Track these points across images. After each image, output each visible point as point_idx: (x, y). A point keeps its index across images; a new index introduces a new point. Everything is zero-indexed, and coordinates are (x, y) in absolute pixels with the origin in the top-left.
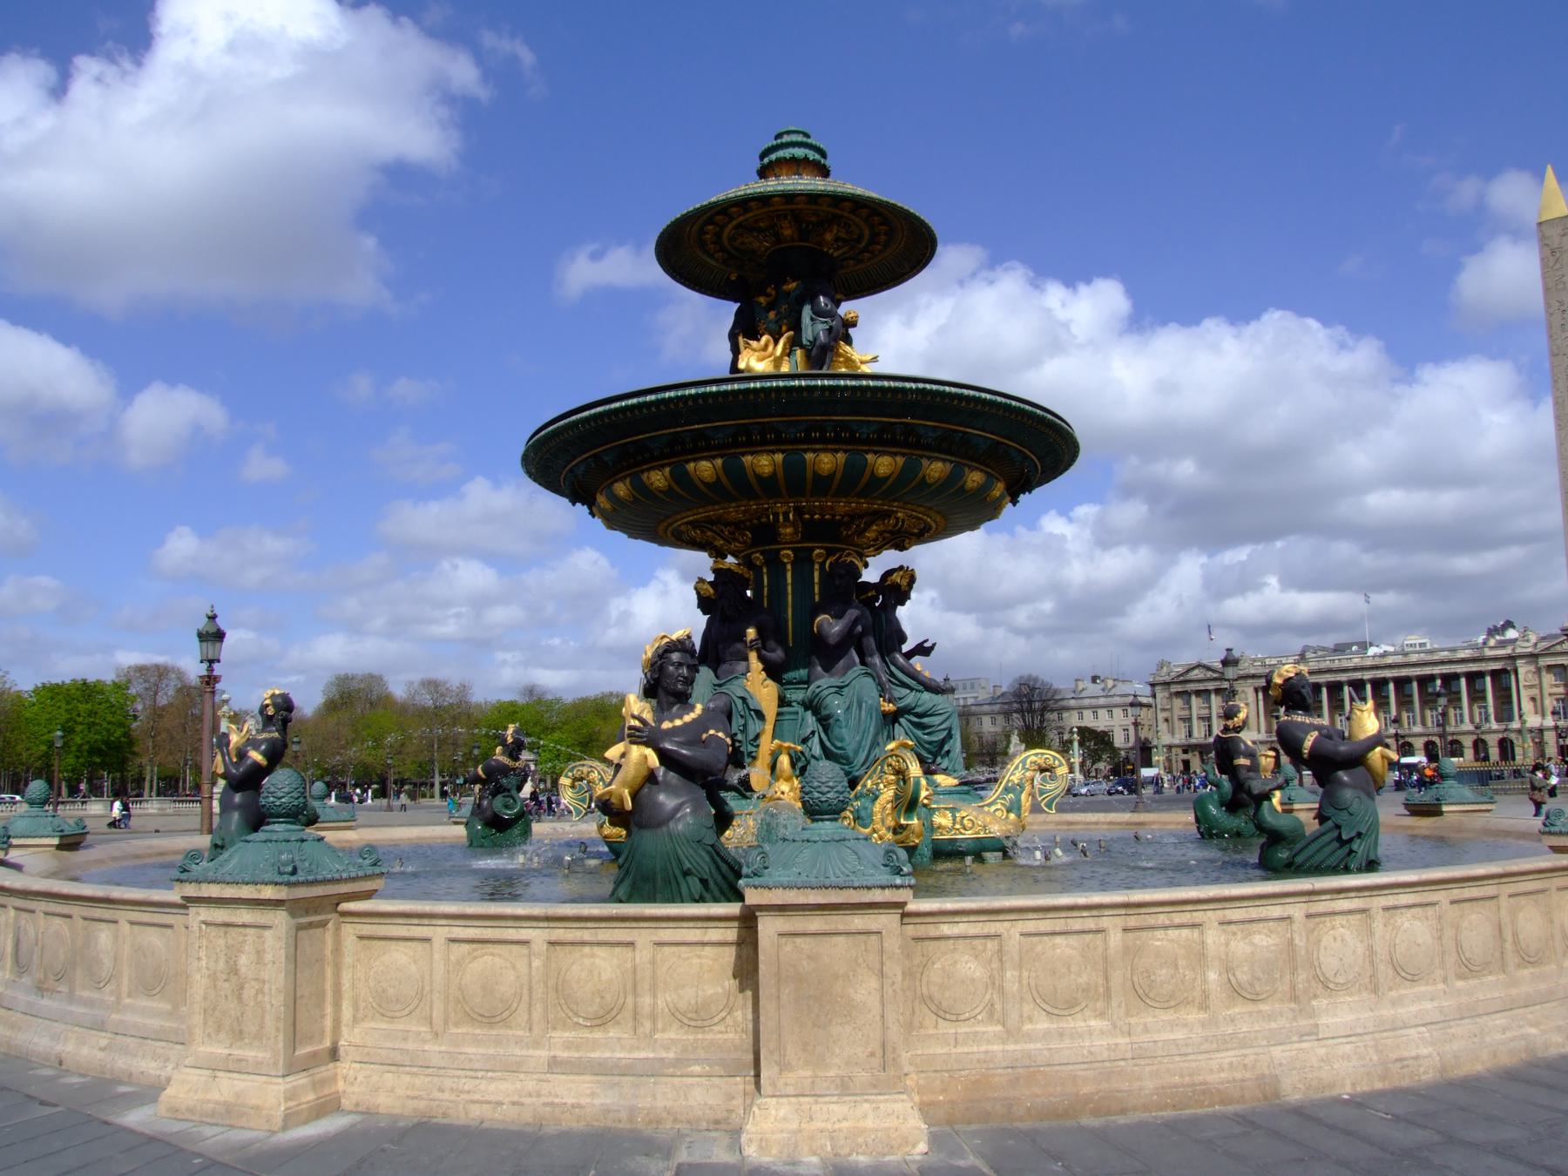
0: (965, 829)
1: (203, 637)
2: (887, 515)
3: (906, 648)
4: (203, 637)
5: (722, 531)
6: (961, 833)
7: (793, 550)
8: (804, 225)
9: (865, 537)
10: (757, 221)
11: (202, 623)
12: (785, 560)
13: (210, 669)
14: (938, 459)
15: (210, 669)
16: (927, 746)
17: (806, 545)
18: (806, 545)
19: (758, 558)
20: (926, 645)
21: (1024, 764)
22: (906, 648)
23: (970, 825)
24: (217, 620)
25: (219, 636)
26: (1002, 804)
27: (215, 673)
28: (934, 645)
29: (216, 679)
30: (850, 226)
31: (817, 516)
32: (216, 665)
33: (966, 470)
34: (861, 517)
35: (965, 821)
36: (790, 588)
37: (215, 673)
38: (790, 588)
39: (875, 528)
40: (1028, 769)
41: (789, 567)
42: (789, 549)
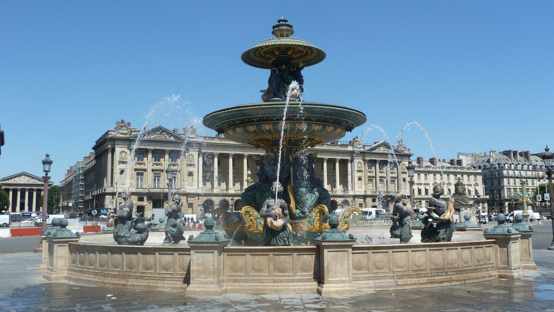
1: (45, 163)
4: (45, 163)
11: (44, 158)
13: (46, 174)
15: (46, 174)
19: (275, 150)
24: (49, 156)
25: (50, 163)
27: (48, 176)
29: (49, 178)
32: (49, 173)
33: (337, 128)
36: (285, 158)
37: (48, 176)
38: (285, 158)
41: (285, 153)
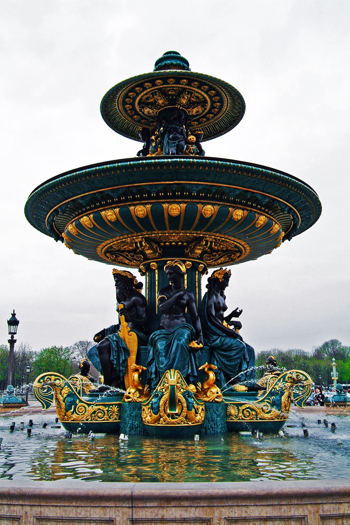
0: (245, 417)
2: (201, 239)
3: (226, 314)
5: (127, 255)
6: (243, 419)
7: (157, 262)
8: (170, 97)
9: (194, 253)
10: (147, 99)
12: (154, 268)
14: (209, 204)
16: (229, 367)
17: (163, 259)
18: (163, 259)
20: (238, 311)
21: (284, 379)
22: (226, 314)
23: (248, 414)
26: (267, 402)
28: (242, 310)
30: (192, 93)
31: (167, 244)
34: (191, 242)
35: (245, 412)
39: (198, 247)
40: (287, 382)
41: (156, 271)
42: (154, 262)
